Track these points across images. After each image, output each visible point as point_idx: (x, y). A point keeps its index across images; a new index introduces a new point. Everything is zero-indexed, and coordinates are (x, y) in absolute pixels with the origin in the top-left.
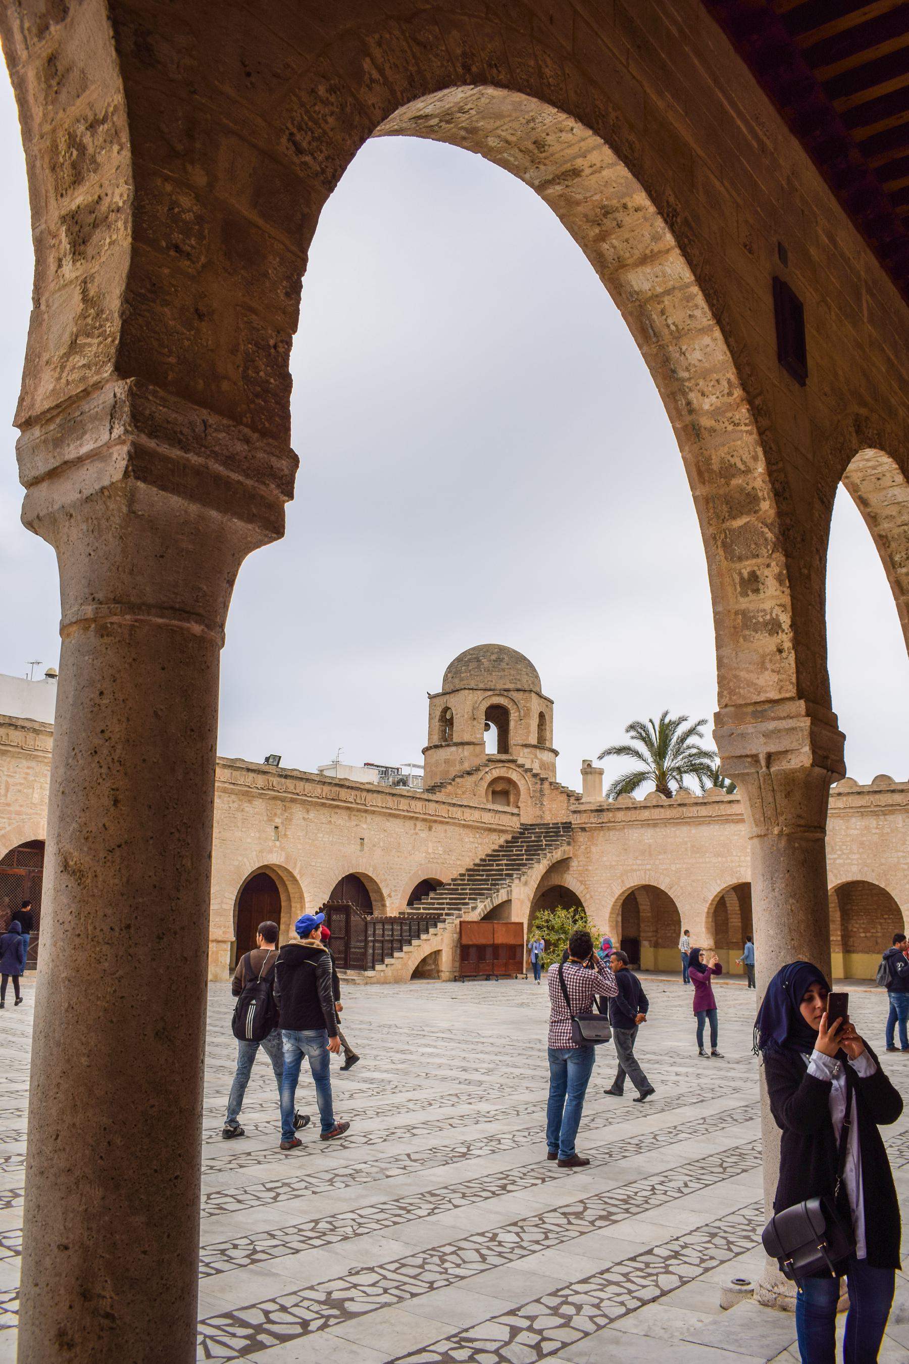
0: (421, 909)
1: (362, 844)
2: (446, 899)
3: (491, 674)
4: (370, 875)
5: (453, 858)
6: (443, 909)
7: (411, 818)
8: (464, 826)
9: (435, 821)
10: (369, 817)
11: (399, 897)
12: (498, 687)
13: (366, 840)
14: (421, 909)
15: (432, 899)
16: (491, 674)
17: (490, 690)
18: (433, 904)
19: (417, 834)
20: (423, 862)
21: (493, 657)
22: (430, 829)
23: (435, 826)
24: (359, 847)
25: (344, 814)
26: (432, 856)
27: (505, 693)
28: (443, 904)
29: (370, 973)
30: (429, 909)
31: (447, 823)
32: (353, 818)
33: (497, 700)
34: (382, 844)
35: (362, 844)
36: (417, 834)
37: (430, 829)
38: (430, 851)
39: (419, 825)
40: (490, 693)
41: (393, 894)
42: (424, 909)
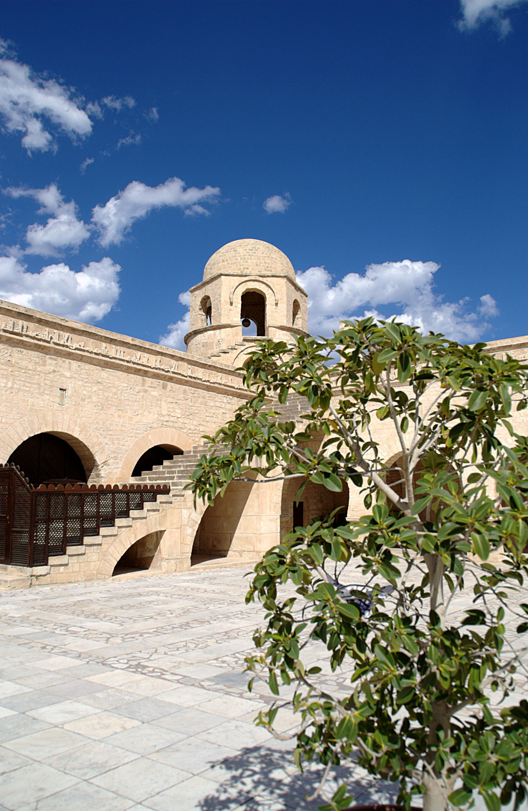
0: (148, 479)
1: (62, 397)
2: (180, 466)
3: (247, 262)
4: (76, 435)
5: (195, 423)
6: (172, 478)
7: (137, 372)
8: (209, 389)
9: (171, 379)
10: (75, 364)
11: (120, 465)
12: (253, 273)
13: (69, 393)
14: (148, 479)
15: (164, 468)
16: (247, 262)
17: (246, 276)
18: (164, 473)
19: (146, 391)
20: (155, 425)
21: (249, 247)
22: (164, 387)
23: (170, 384)
24: (58, 400)
25: (34, 355)
26: (166, 418)
27: (261, 279)
28: (173, 472)
29: (39, 570)
30: (156, 479)
31: (187, 382)
32: (49, 361)
33: (252, 285)
34: (94, 399)
35: (62, 397)
36: (146, 391)
37: (164, 387)
38: (165, 412)
39: (149, 380)
40: (245, 279)
41: (111, 461)
42: (150, 479)
